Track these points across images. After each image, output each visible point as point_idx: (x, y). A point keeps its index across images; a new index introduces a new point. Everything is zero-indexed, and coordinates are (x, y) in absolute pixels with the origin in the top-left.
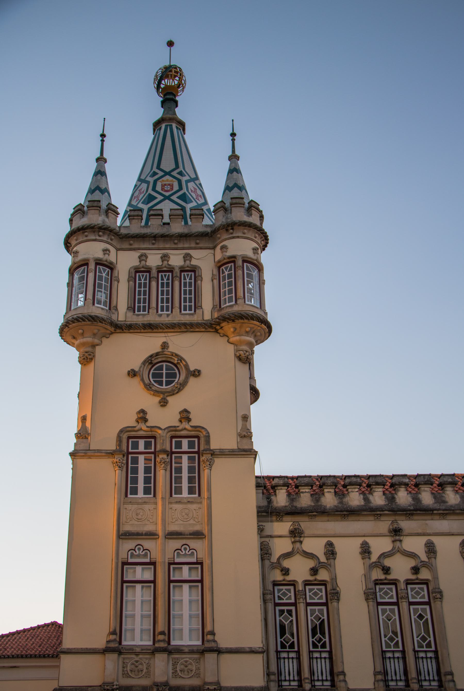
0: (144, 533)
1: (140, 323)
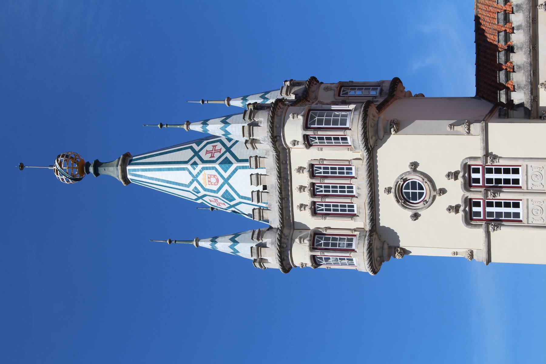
1: (368, 212)
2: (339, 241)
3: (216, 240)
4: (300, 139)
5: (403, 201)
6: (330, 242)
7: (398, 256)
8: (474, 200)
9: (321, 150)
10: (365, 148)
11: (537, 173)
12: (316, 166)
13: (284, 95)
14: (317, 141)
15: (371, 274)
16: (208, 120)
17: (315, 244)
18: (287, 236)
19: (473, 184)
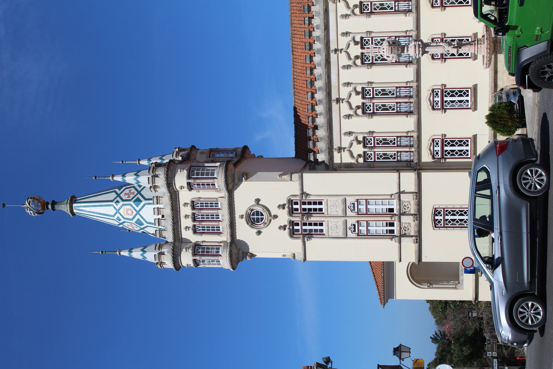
0: (343, 226)
1: (229, 230)
2: (211, 249)
3: (132, 251)
4: (185, 185)
5: (251, 223)
6: (205, 250)
7: (248, 258)
8: (295, 222)
9: (199, 192)
10: (226, 190)
11: (334, 204)
12: (195, 202)
13: (175, 157)
14: (196, 186)
15: (231, 270)
16: (126, 174)
17: (196, 252)
18: (177, 247)
19: (294, 212)
